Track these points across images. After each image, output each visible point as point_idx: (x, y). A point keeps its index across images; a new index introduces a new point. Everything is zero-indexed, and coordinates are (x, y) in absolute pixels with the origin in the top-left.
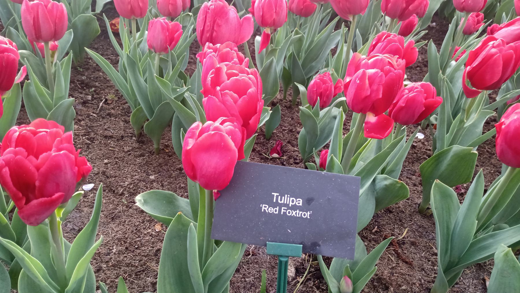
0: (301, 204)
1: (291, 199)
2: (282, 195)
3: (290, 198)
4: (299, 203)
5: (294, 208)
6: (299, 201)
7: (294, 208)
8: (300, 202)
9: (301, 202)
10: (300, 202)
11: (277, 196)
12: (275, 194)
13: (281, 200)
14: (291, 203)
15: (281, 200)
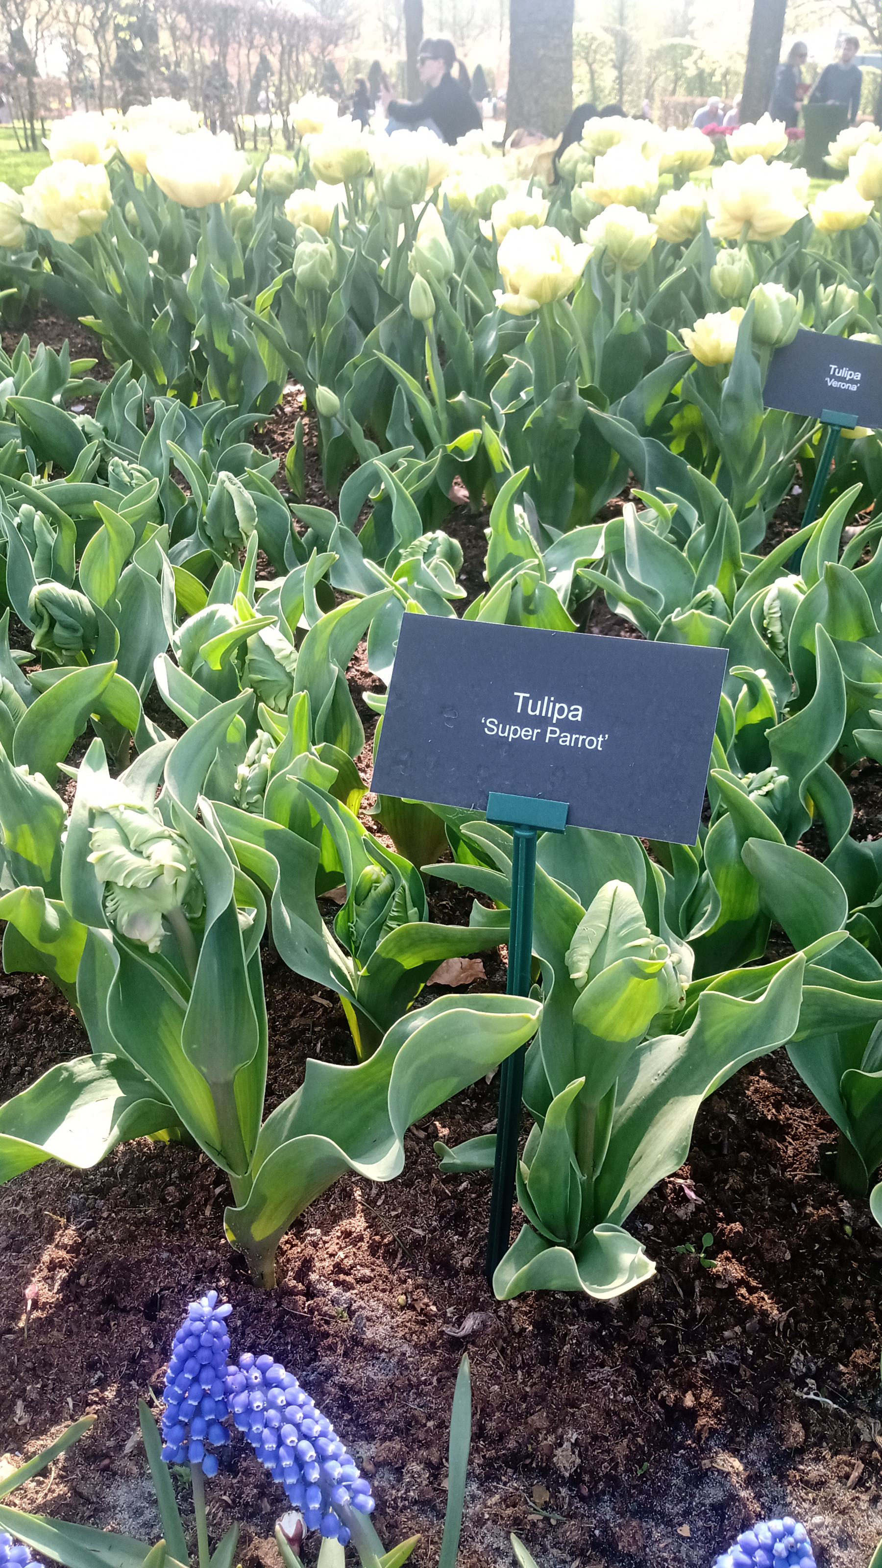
0: (579, 718)
1: (558, 706)
2: (537, 697)
3: (555, 703)
4: (573, 716)
5: (566, 726)
6: (577, 710)
7: (566, 726)
8: (577, 713)
9: (580, 713)
10: (577, 713)
11: (526, 700)
12: (522, 695)
13: (534, 710)
14: (556, 715)
15: (534, 710)
